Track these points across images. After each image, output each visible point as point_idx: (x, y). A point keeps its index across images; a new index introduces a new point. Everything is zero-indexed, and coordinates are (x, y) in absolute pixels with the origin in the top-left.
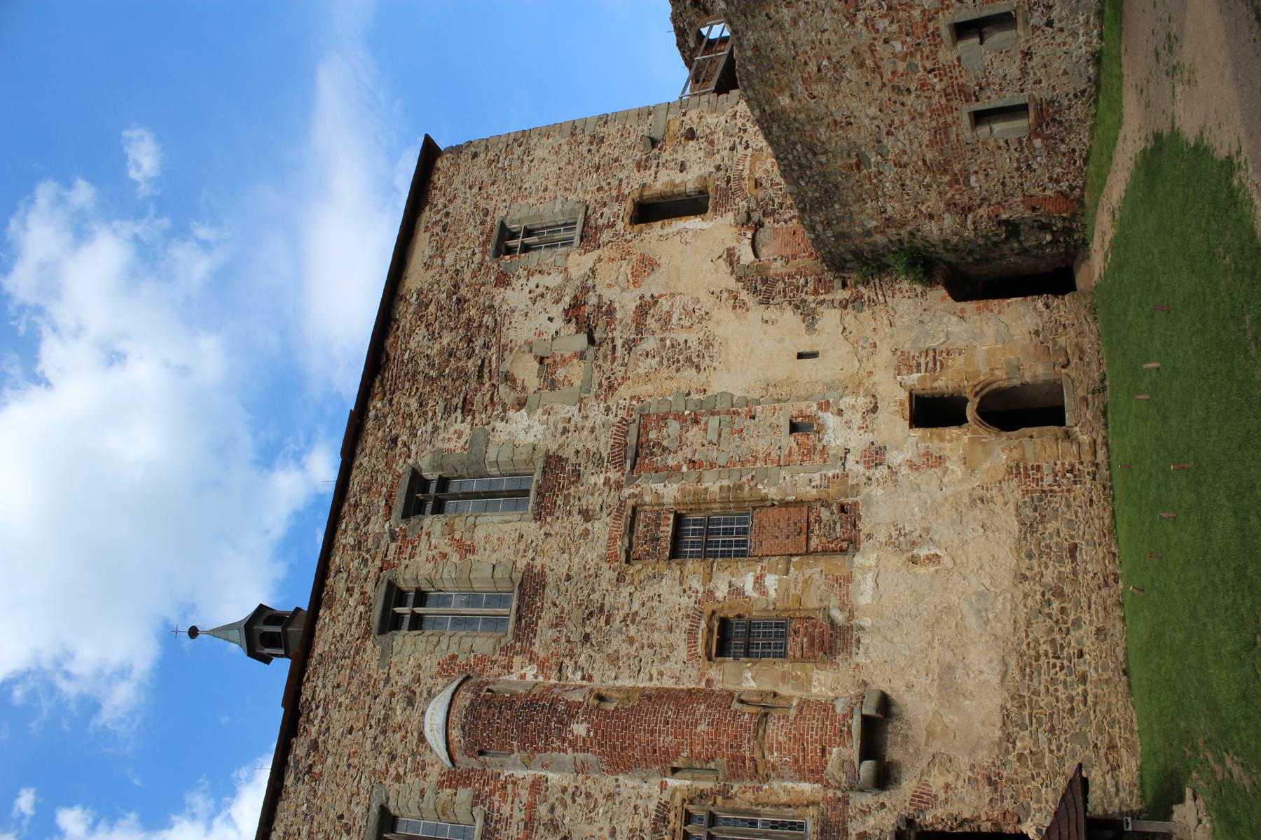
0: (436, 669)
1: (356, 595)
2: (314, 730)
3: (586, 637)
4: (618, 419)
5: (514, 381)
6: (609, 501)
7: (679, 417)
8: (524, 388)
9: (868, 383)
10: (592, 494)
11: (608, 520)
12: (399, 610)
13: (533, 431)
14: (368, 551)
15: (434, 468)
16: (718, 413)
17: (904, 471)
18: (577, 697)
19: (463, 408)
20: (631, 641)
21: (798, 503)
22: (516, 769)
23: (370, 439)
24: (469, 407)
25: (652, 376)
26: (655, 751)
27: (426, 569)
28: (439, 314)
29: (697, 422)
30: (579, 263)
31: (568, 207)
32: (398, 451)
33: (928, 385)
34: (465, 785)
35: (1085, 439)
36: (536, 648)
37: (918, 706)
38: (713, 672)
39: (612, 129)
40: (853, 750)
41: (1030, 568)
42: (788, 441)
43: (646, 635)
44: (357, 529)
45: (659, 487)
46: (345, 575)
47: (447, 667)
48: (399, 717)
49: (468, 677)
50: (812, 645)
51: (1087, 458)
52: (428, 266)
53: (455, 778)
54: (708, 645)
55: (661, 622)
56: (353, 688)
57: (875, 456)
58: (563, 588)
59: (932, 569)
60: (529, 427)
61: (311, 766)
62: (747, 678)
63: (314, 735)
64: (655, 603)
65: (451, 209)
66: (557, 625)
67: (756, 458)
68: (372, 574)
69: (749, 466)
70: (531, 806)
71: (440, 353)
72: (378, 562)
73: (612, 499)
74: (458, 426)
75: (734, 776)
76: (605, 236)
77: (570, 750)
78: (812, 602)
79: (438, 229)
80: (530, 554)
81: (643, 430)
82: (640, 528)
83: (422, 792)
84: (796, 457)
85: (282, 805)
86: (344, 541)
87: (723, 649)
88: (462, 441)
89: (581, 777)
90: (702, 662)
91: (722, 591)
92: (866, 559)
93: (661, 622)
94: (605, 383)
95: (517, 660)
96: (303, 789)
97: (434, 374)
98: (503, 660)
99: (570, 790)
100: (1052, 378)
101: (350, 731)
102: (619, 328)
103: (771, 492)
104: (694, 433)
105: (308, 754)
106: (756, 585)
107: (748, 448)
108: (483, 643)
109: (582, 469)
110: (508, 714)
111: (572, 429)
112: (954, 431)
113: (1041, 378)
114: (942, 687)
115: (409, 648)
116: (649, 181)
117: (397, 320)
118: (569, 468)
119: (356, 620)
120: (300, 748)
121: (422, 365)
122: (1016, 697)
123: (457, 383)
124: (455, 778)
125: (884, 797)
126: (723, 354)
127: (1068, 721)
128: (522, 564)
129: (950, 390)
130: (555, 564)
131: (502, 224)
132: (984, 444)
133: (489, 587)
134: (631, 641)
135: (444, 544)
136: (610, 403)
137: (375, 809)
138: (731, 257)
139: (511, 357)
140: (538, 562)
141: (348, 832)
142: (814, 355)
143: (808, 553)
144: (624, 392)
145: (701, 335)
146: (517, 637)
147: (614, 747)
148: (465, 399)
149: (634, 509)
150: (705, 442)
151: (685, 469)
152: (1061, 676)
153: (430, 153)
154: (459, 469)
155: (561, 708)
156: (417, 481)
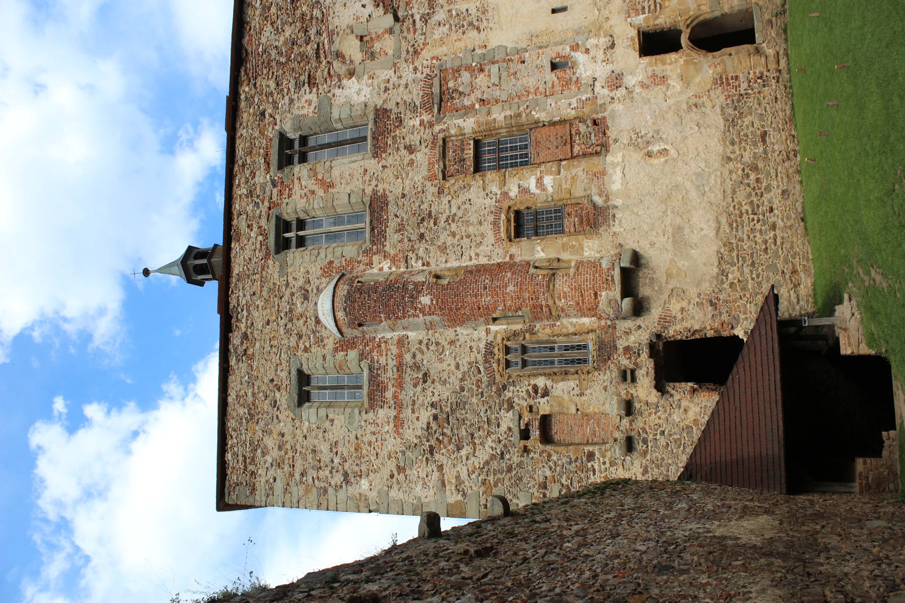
0: (320, 272)
1: (255, 229)
2: (243, 326)
3: (422, 236)
4: (424, 75)
5: (343, 57)
6: (425, 137)
7: (469, 68)
8: (351, 61)
9: (606, 26)
10: (413, 133)
11: (426, 150)
12: (287, 235)
13: (363, 93)
14: (258, 196)
15: (295, 130)
16: (497, 62)
17: (638, 90)
18: (420, 278)
19: (309, 83)
20: (454, 235)
21: (562, 122)
22: (386, 332)
23: (245, 115)
24: (313, 81)
25: (445, 40)
26: (479, 308)
27: (301, 204)
28: (279, 13)
29: (482, 70)
32: (267, 121)
33: (651, 23)
34: (352, 348)
35: (770, 52)
36: (387, 249)
37: (659, 257)
38: (514, 249)
40: (616, 291)
41: (733, 152)
42: (550, 77)
43: (463, 229)
44: (247, 182)
45: (460, 122)
46: (245, 217)
47: (327, 270)
48: (299, 309)
49: (343, 275)
50: (581, 223)
51: (772, 66)
53: (345, 345)
54: (508, 231)
55: (474, 219)
56: (265, 294)
57: (616, 81)
58: (400, 204)
59: (663, 160)
60: (360, 90)
61: (245, 350)
62: (538, 251)
63: (244, 330)
64: (467, 206)
66: (400, 230)
67: (529, 92)
68: (263, 213)
69: (524, 99)
70: (400, 356)
71: (285, 43)
72: (266, 204)
73: (427, 135)
74: (308, 97)
75: (536, 318)
77: (421, 315)
78: (578, 192)
80: (374, 183)
81: (443, 82)
82: (450, 154)
83: (324, 358)
84: (558, 88)
85: (231, 378)
86: (239, 193)
87: (519, 233)
89: (430, 332)
90: (506, 243)
91: (514, 192)
92: (615, 157)
93: (474, 219)
94: (411, 50)
95: (376, 258)
96: (243, 366)
97: (283, 60)
98: (365, 260)
99: (425, 342)
100: (744, 7)
101: (268, 323)
102: (416, 6)
103: (541, 116)
104: (481, 79)
105: (242, 343)
106: (538, 185)
107: (522, 86)
108: (350, 250)
109: (402, 116)
110: (374, 296)
111: (391, 87)
112: (673, 56)
113: (736, 9)
114: (675, 242)
115: (298, 261)
117: (248, 23)
118: (393, 116)
119: (258, 246)
120: (235, 339)
121: (273, 54)
122: (727, 244)
123: (302, 65)
124: (345, 345)
125: (639, 321)
126: (496, 17)
127: (764, 257)
128: (369, 190)
129: (668, 26)
130: (392, 187)
132: (695, 64)
134: (454, 235)
135: (311, 184)
136: (416, 64)
137: (294, 373)
139: (339, 39)
140: (380, 188)
141: (279, 390)
142: (564, 9)
143: (573, 157)
144: (426, 55)
145: (478, 4)
146: (373, 243)
147: (451, 309)
148: (309, 76)
149: (444, 140)
150: (490, 85)
151: (477, 106)
152: (758, 226)
154: (313, 128)
155: (411, 287)
156: (284, 141)
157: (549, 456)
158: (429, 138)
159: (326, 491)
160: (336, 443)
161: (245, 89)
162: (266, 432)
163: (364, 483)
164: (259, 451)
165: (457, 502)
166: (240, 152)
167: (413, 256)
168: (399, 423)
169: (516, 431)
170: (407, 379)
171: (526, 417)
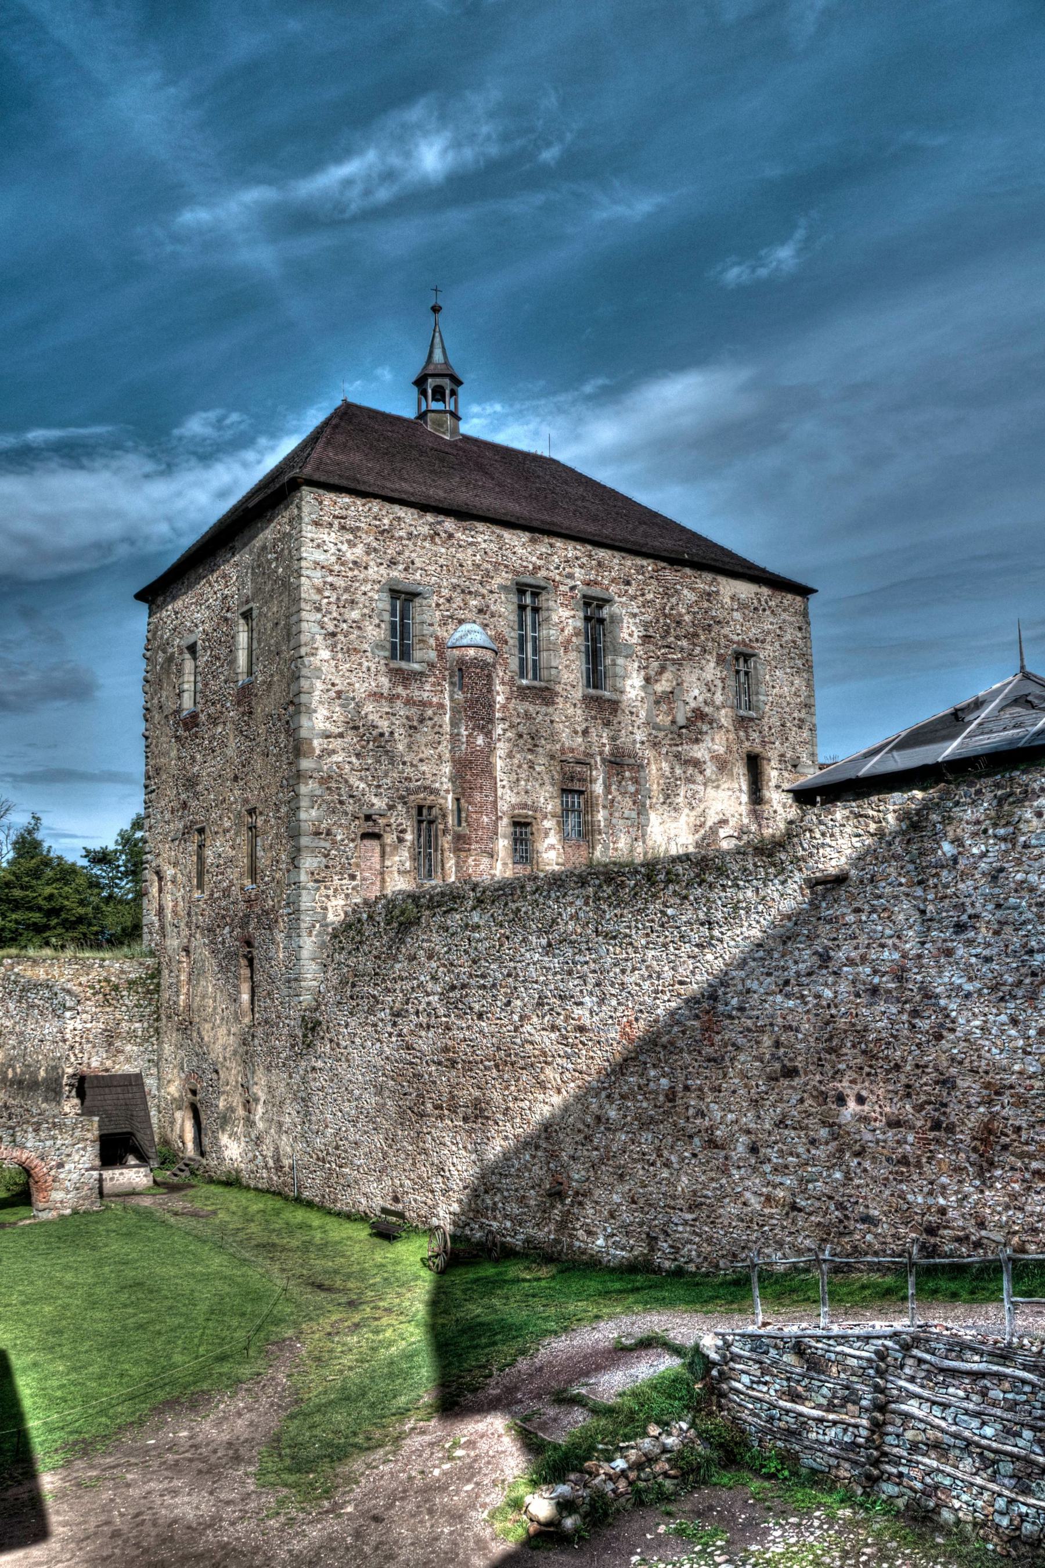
3: (520, 736)
12: (528, 594)
23: (629, 563)
27: (555, 618)
29: (634, 803)
30: (725, 716)
31: (761, 705)
38: (505, 821)
39: (806, 734)
45: (600, 781)
52: (733, 598)
53: (441, 647)
54: (519, 815)
56: (486, 565)
65: (768, 612)
70: (430, 704)
72: (558, 578)
75: (459, 838)
76: (742, 733)
79: (756, 604)
83: (431, 625)
87: (516, 824)
88: (627, 637)
96: (425, 530)
98: (507, 678)
101: (461, 566)
108: (514, 664)
116: (772, 763)
120: (449, 524)
128: (558, 688)
131: (754, 655)
133: (543, 663)
134: (520, 767)
138: (724, 822)
140: (559, 700)
141: (406, 569)
144: (649, 753)
146: (521, 688)
153: (804, 591)
157: (353, 840)
158: (591, 752)
159: (318, 610)
160: (359, 628)
161: (649, 565)
162: (369, 550)
163: (325, 654)
164: (351, 537)
165: (314, 749)
166: (602, 554)
167: (506, 726)
168: (376, 696)
169: (372, 811)
170: (414, 710)
171: (382, 821)
